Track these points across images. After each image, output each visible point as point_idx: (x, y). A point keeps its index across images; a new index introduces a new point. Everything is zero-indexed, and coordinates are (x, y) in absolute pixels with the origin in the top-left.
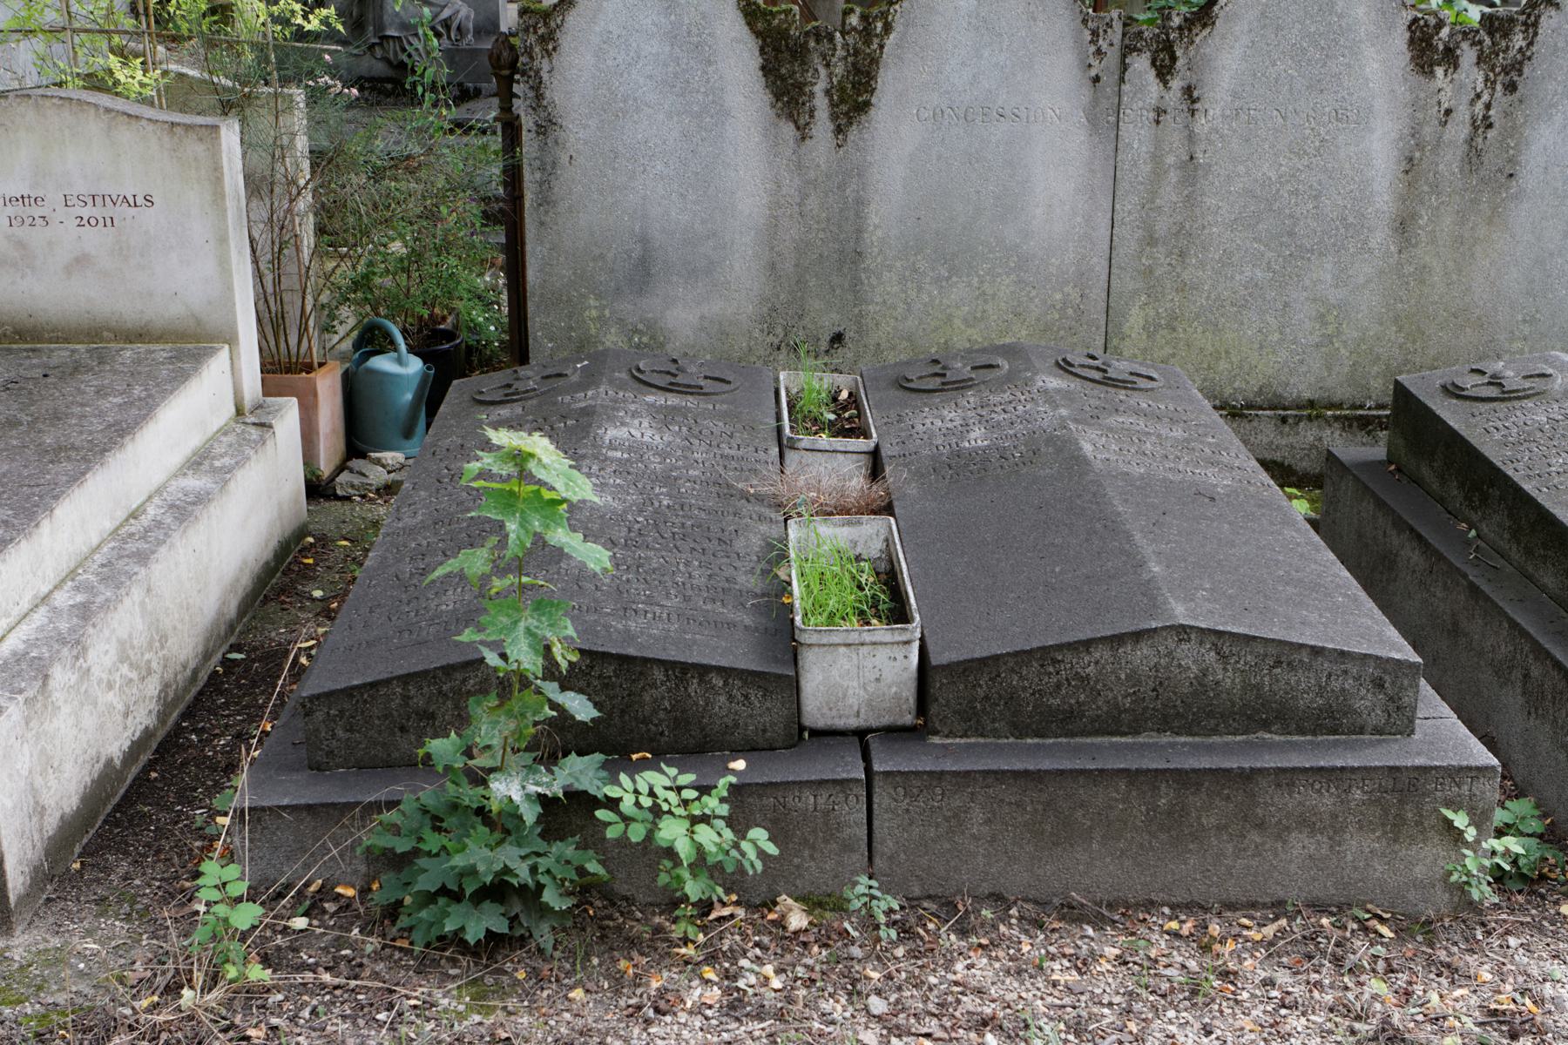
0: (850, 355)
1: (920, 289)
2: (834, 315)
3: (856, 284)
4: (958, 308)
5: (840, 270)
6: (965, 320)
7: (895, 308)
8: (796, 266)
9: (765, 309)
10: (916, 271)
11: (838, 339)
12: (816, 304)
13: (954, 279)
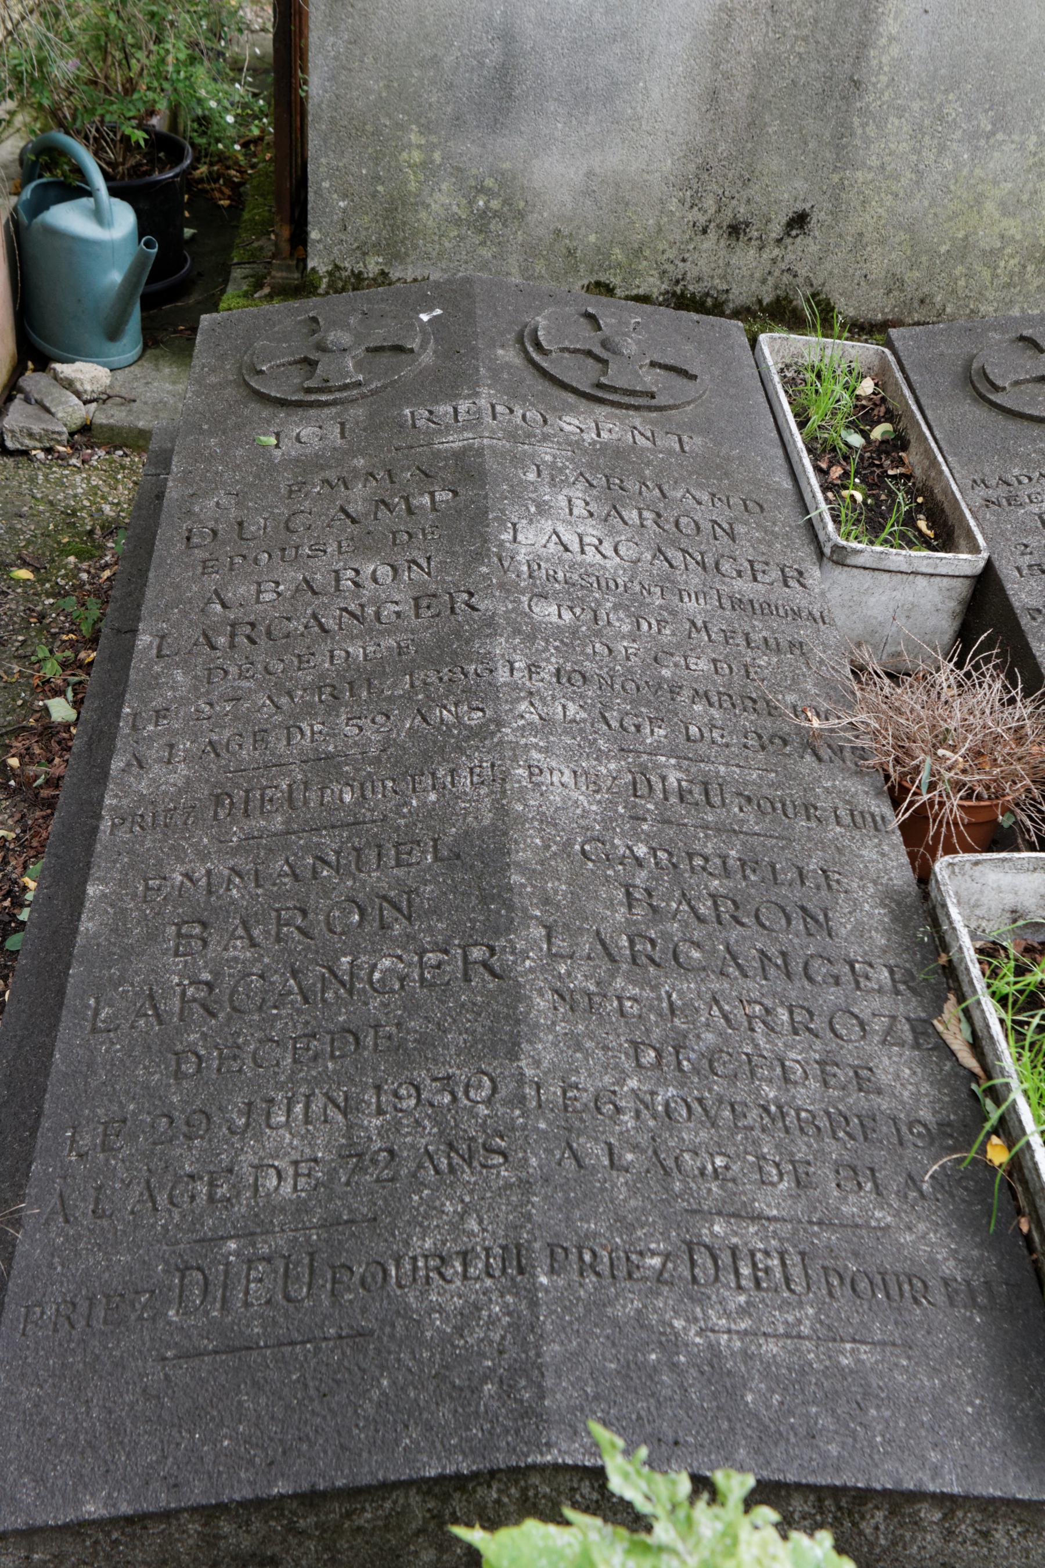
0: (814, 248)
1: (942, 149)
2: (799, 184)
3: (843, 132)
4: (995, 183)
5: (821, 108)
6: (1003, 205)
7: (897, 178)
8: (752, 97)
9: (692, 167)
10: (941, 119)
11: (799, 221)
12: (774, 163)
13: (1000, 136)
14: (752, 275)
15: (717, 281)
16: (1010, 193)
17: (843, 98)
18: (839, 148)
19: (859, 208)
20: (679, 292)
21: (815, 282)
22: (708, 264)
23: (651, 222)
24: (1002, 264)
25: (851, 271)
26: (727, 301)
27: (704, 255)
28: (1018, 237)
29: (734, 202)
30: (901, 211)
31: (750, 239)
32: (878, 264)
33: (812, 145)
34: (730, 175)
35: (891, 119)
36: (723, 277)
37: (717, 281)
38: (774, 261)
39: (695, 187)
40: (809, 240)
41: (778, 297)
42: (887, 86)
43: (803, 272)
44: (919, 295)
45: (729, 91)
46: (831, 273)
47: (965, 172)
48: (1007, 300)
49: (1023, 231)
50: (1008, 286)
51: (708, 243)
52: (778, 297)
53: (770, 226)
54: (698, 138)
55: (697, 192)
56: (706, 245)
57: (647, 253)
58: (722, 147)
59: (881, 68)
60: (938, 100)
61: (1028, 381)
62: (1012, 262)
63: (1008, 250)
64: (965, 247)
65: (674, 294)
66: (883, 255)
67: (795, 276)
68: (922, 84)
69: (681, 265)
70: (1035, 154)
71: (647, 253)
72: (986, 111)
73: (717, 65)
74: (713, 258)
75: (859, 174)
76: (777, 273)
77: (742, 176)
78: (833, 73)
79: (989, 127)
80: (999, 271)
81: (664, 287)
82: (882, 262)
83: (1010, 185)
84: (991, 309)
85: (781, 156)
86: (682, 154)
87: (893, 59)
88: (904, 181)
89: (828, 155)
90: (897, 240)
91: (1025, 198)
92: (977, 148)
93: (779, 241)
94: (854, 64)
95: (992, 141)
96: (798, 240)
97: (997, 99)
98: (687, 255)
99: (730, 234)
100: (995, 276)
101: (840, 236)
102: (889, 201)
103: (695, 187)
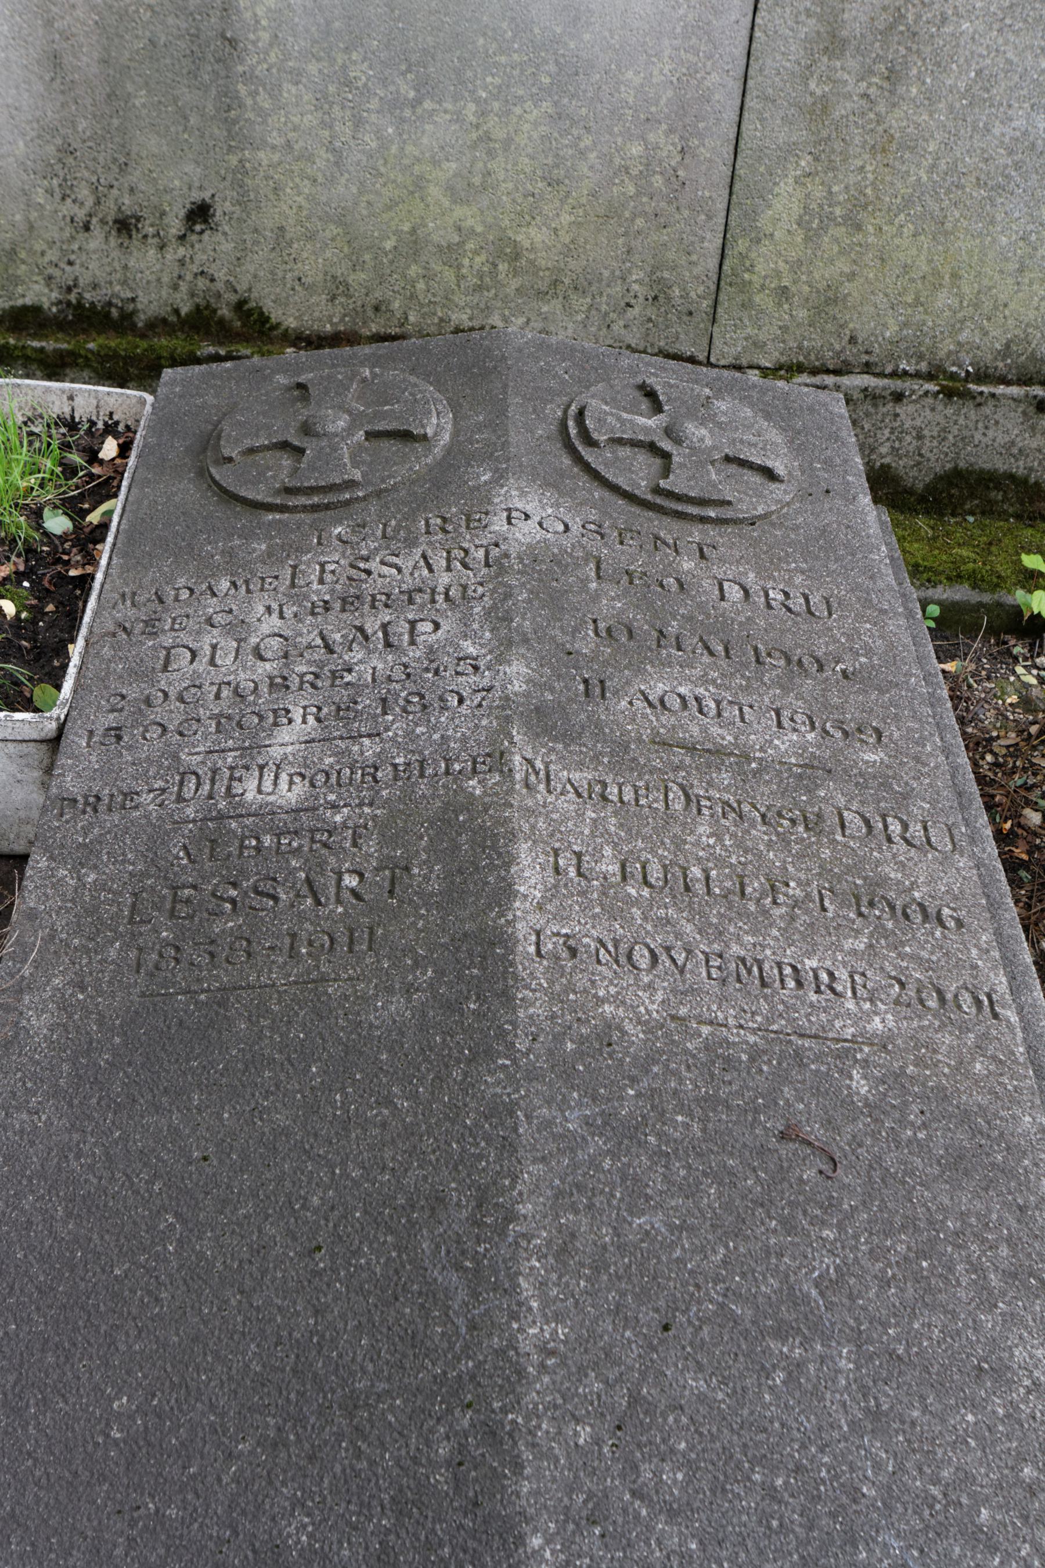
0: (227, 246)
1: (358, 123)
2: (189, 168)
3: (228, 104)
4: (436, 163)
5: (193, 74)
6: (450, 189)
7: (310, 158)
8: (105, 61)
9: (51, 149)
10: (348, 84)
11: (200, 214)
12: (150, 144)
13: (428, 105)
14: (159, 280)
15: (118, 288)
16: (455, 175)
17: (218, 61)
18: (230, 124)
19: (271, 197)
20: (74, 301)
21: (238, 288)
22: (103, 269)
23: (18, 217)
24: (466, 262)
25: (280, 274)
26: (135, 312)
27: (94, 257)
28: (479, 229)
29: (115, 192)
30: (324, 199)
31: (145, 237)
32: (312, 264)
33: (193, 121)
34: (101, 159)
35: (285, 85)
36: (124, 283)
37: (118, 288)
38: (182, 262)
39: (61, 174)
40: (219, 237)
41: (198, 306)
42: (271, 45)
43: (221, 275)
44: (371, 300)
45: (75, 56)
46: (255, 276)
47: (394, 149)
48: (482, 306)
49: (483, 222)
50: (479, 288)
51: (96, 241)
52: (198, 306)
53: (166, 221)
54: (49, 114)
55: (65, 180)
56: (93, 245)
57: (23, 255)
58: (82, 124)
59: (257, 22)
60: (340, 61)
61: (267, 448)
62: (478, 260)
63: (470, 246)
64: (415, 242)
65: (69, 304)
66: (314, 253)
67: (212, 280)
68: (315, 42)
69: (68, 268)
70: (477, 127)
71: (23, 255)
72: (403, 74)
73: (49, 23)
74: (106, 261)
75: (261, 154)
76: (189, 277)
77: (115, 160)
78: (198, 29)
79: (412, 94)
80: (464, 271)
81: (55, 295)
82: (316, 261)
83: (454, 165)
84: (465, 317)
85: (158, 133)
86: (34, 134)
87: (269, 10)
88: (320, 163)
89: (216, 131)
90: (328, 234)
91: (477, 180)
92: (403, 120)
93: (182, 238)
94: (222, 18)
95: (419, 111)
96: (206, 236)
97: (414, 58)
98: (73, 257)
99: (119, 230)
100: (460, 277)
101: (256, 230)
102: (306, 188)
103: (61, 174)
